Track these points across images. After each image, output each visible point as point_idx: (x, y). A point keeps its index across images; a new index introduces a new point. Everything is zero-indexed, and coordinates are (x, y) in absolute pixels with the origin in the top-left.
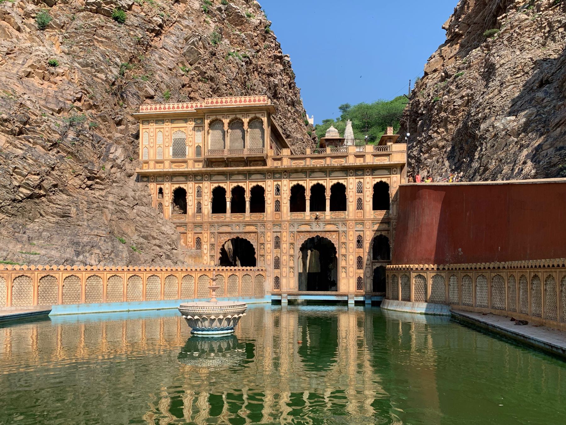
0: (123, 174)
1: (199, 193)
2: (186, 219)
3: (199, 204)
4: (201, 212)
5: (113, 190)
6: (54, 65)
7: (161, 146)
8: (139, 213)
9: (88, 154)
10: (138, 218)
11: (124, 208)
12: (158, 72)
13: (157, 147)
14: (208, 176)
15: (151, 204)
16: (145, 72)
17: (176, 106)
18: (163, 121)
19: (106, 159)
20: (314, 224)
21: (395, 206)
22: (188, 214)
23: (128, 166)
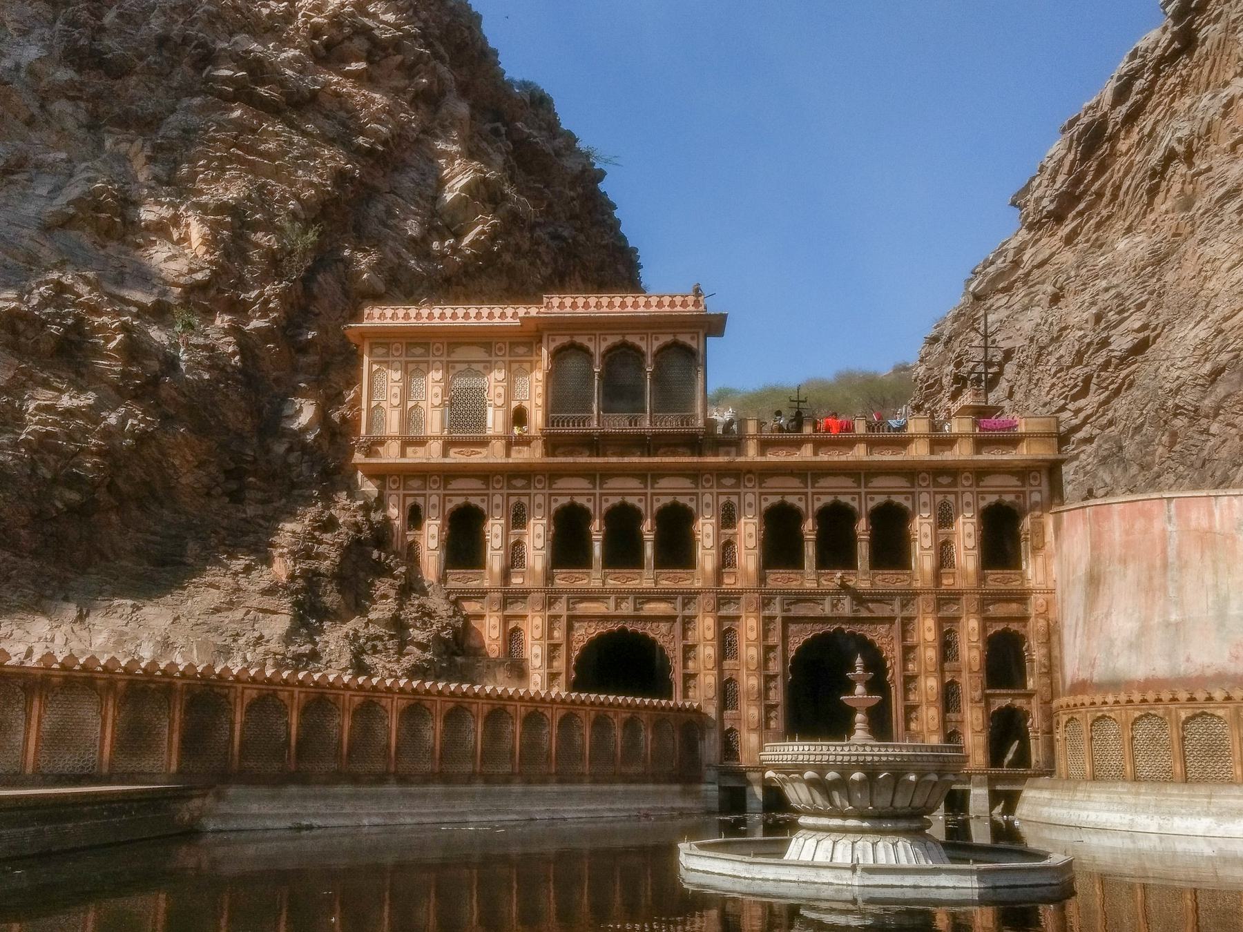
9: (230, 414)
12: (391, 243)
22: (491, 569)
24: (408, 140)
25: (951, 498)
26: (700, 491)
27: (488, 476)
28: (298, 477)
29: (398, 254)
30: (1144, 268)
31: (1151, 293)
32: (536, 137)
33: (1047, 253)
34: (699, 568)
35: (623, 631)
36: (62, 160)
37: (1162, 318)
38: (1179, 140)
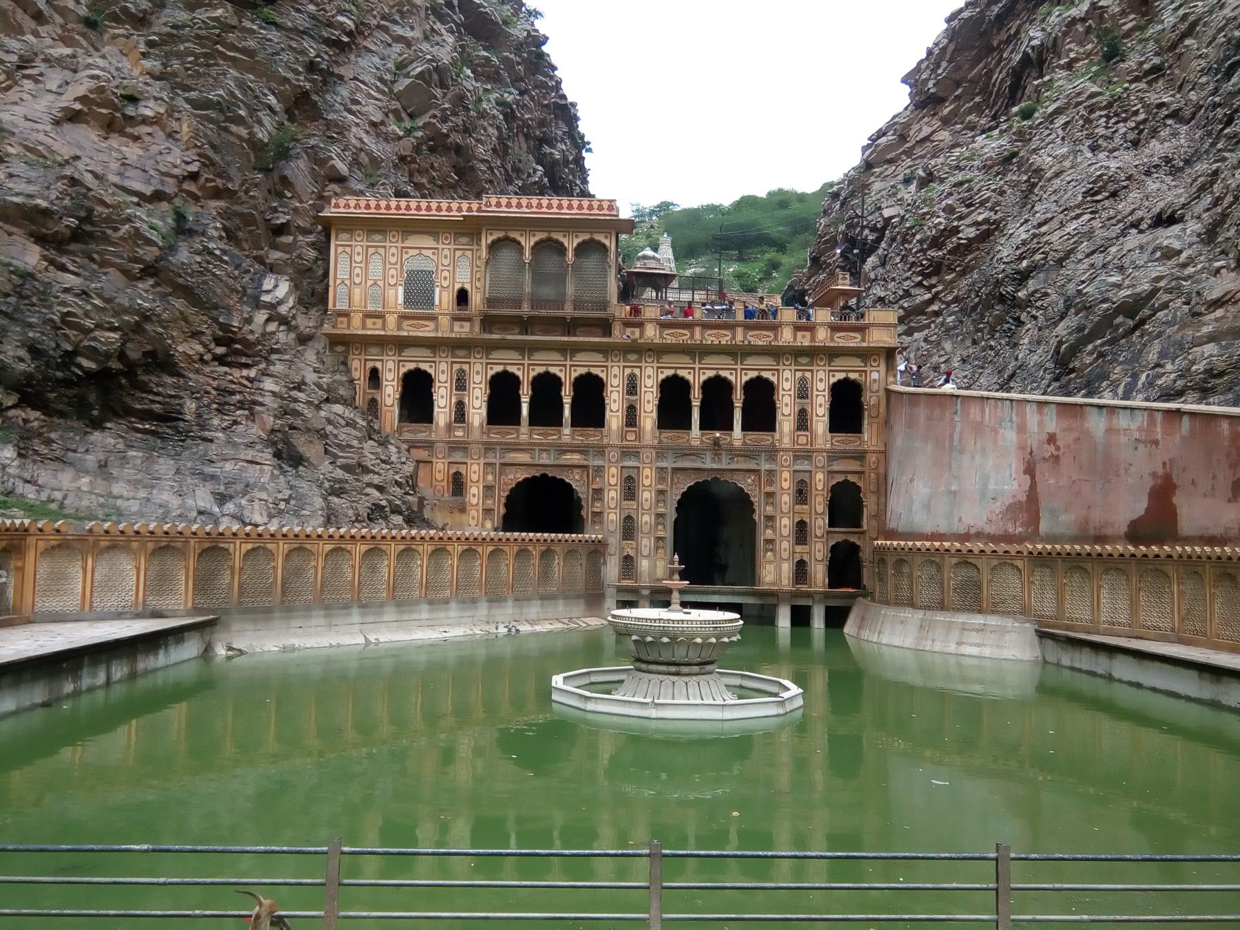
0: (292, 336)
1: (461, 383)
2: (430, 434)
3: (460, 406)
4: (464, 422)
5: (271, 368)
6: (133, 99)
7: (379, 283)
8: (332, 418)
10: (329, 428)
11: (300, 407)
12: (354, 129)
13: (369, 284)
14: (489, 348)
15: (354, 399)
16: (325, 128)
17: (393, 204)
18: (383, 232)
19: (258, 305)
20: (709, 456)
21: (875, 426)
22: (437, 423)
23: (305, 323)
24: (370, 28)
25: (808, 375)
26: (609, 364)
27: (435, 346)
28: (276, 344)
29: (361, 139)
30: (991, 167)
31: (994, 191)
32: (485, 7)
33: (930, 130)
34: (606, 427)
35: (544, 476)
36: (68, 56)
37: (1000, 215)
38: (1033, 48)
